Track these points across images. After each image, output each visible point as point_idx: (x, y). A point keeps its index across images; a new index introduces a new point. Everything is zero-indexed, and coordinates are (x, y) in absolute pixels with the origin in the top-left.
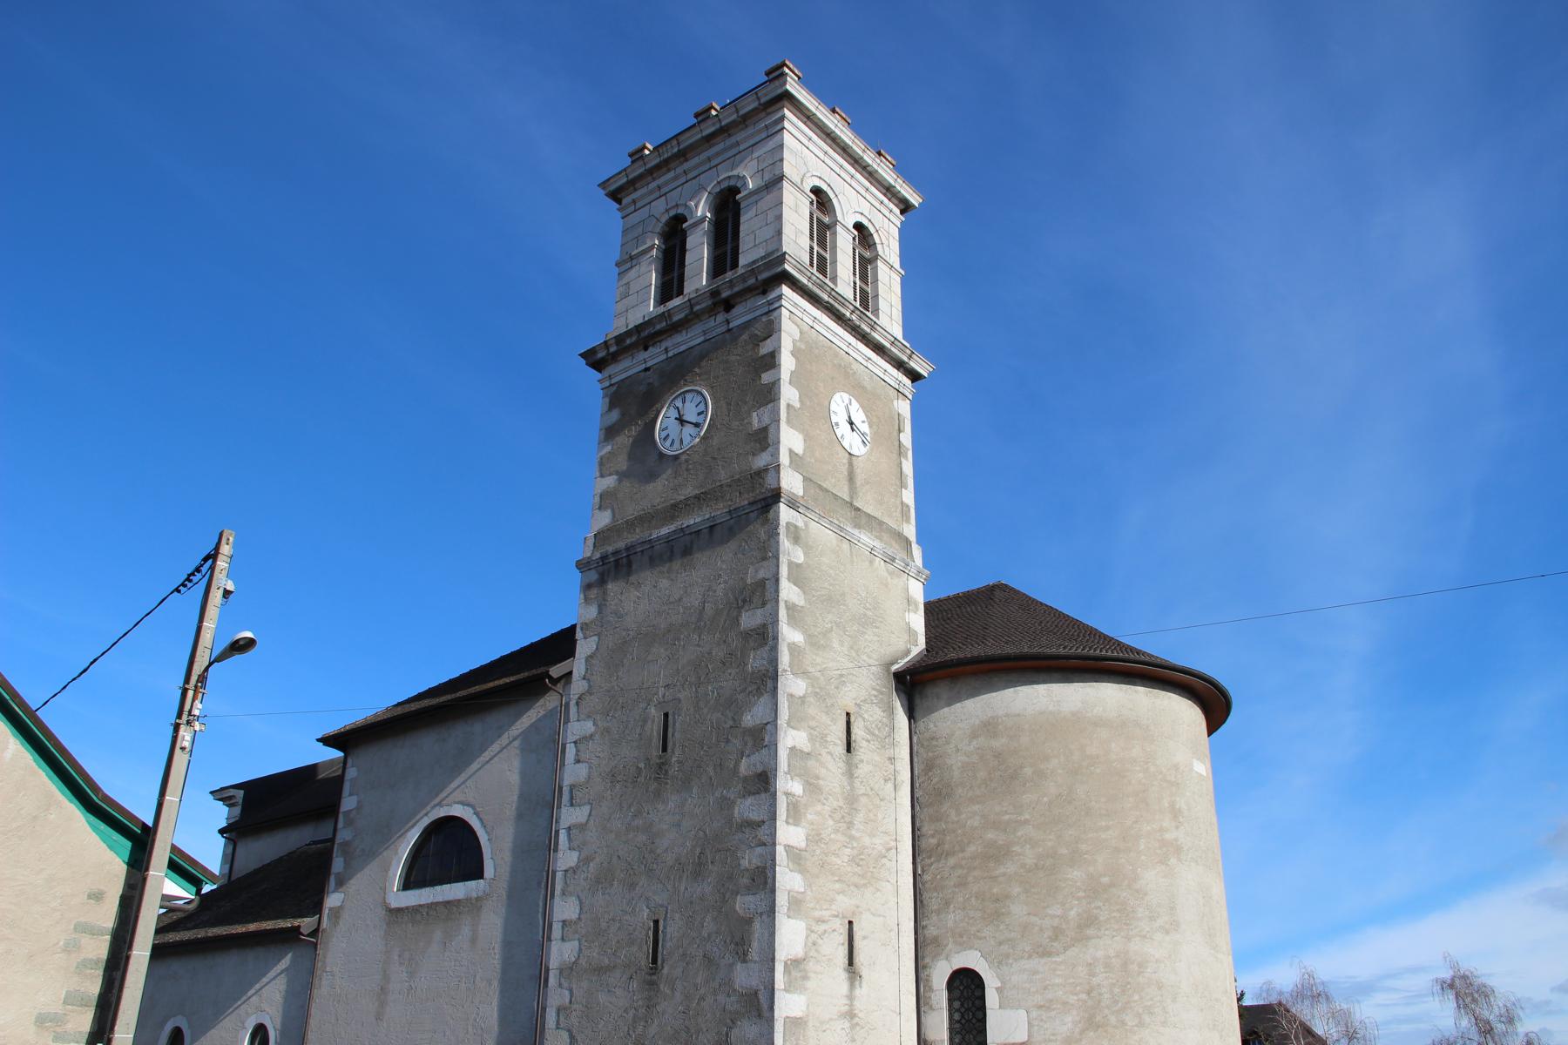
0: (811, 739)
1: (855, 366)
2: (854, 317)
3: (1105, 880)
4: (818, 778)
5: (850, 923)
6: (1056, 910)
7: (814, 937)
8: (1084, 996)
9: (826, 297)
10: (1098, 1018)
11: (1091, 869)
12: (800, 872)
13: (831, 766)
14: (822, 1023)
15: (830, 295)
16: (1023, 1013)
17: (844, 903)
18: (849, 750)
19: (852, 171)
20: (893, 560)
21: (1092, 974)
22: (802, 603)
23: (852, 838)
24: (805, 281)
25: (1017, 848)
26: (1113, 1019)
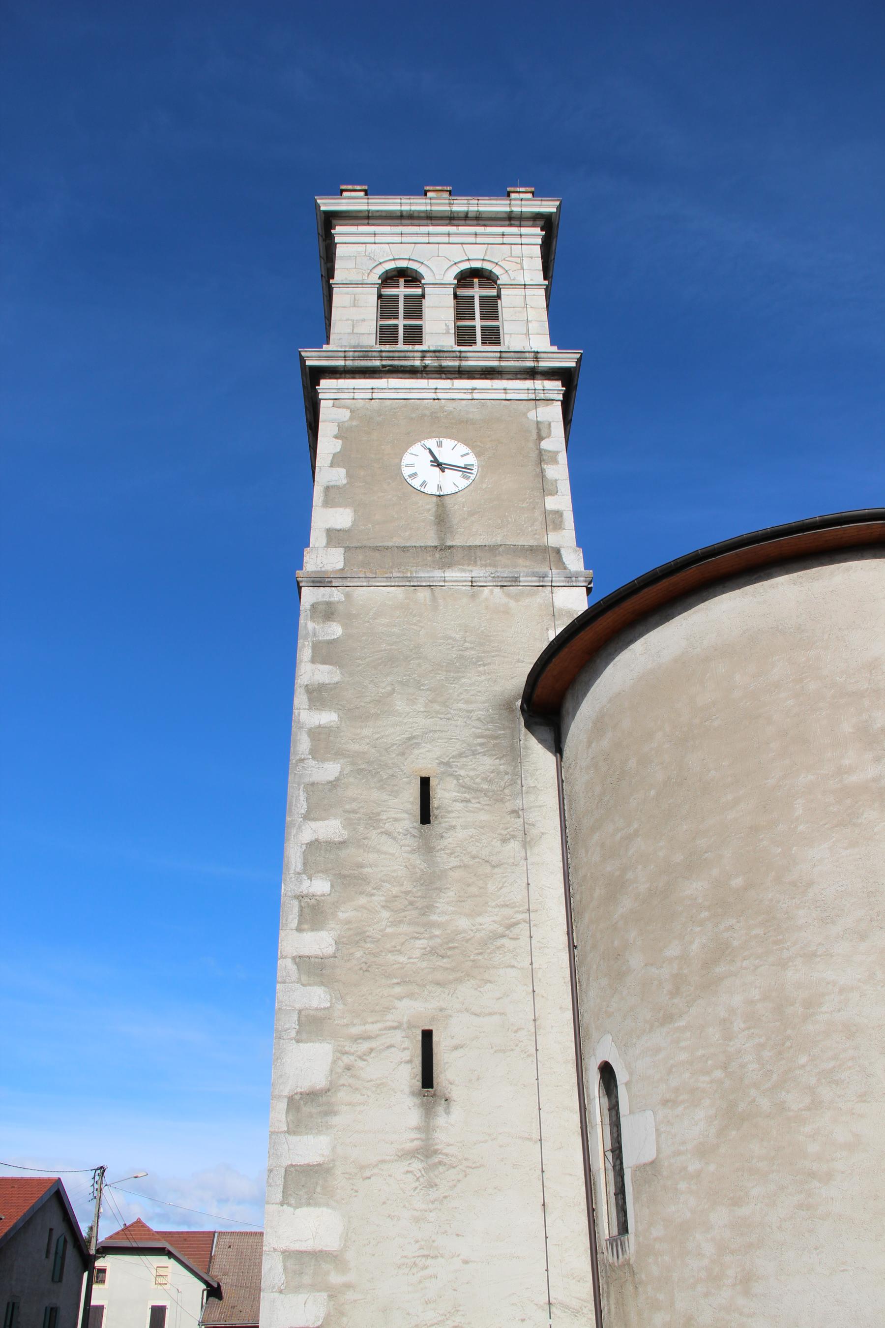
0: (349, 824)
1: (450, 406)
2: (427, 362)
3: (737, 882)
4: (361, 866)
5: (427, 1036)
6: (673, 950)
7: (346, 1059)
8: (719, 1074)
9: (377, 363)
10: (742, 1106)
11: (715, 872)
12: (322, 984)
13: (393, 849)
14: (362, 1168)
15: (381, 358)
16: (649, 1113)
17: (415, 1010)
18: (425, 817)
19: (514, 230)
20: (516, 579)
21: (728, 1037)
22: (337, 677)
23: (432, 925)
24: (341, 363)
25: (630, 875)
26: (765, 1104)
